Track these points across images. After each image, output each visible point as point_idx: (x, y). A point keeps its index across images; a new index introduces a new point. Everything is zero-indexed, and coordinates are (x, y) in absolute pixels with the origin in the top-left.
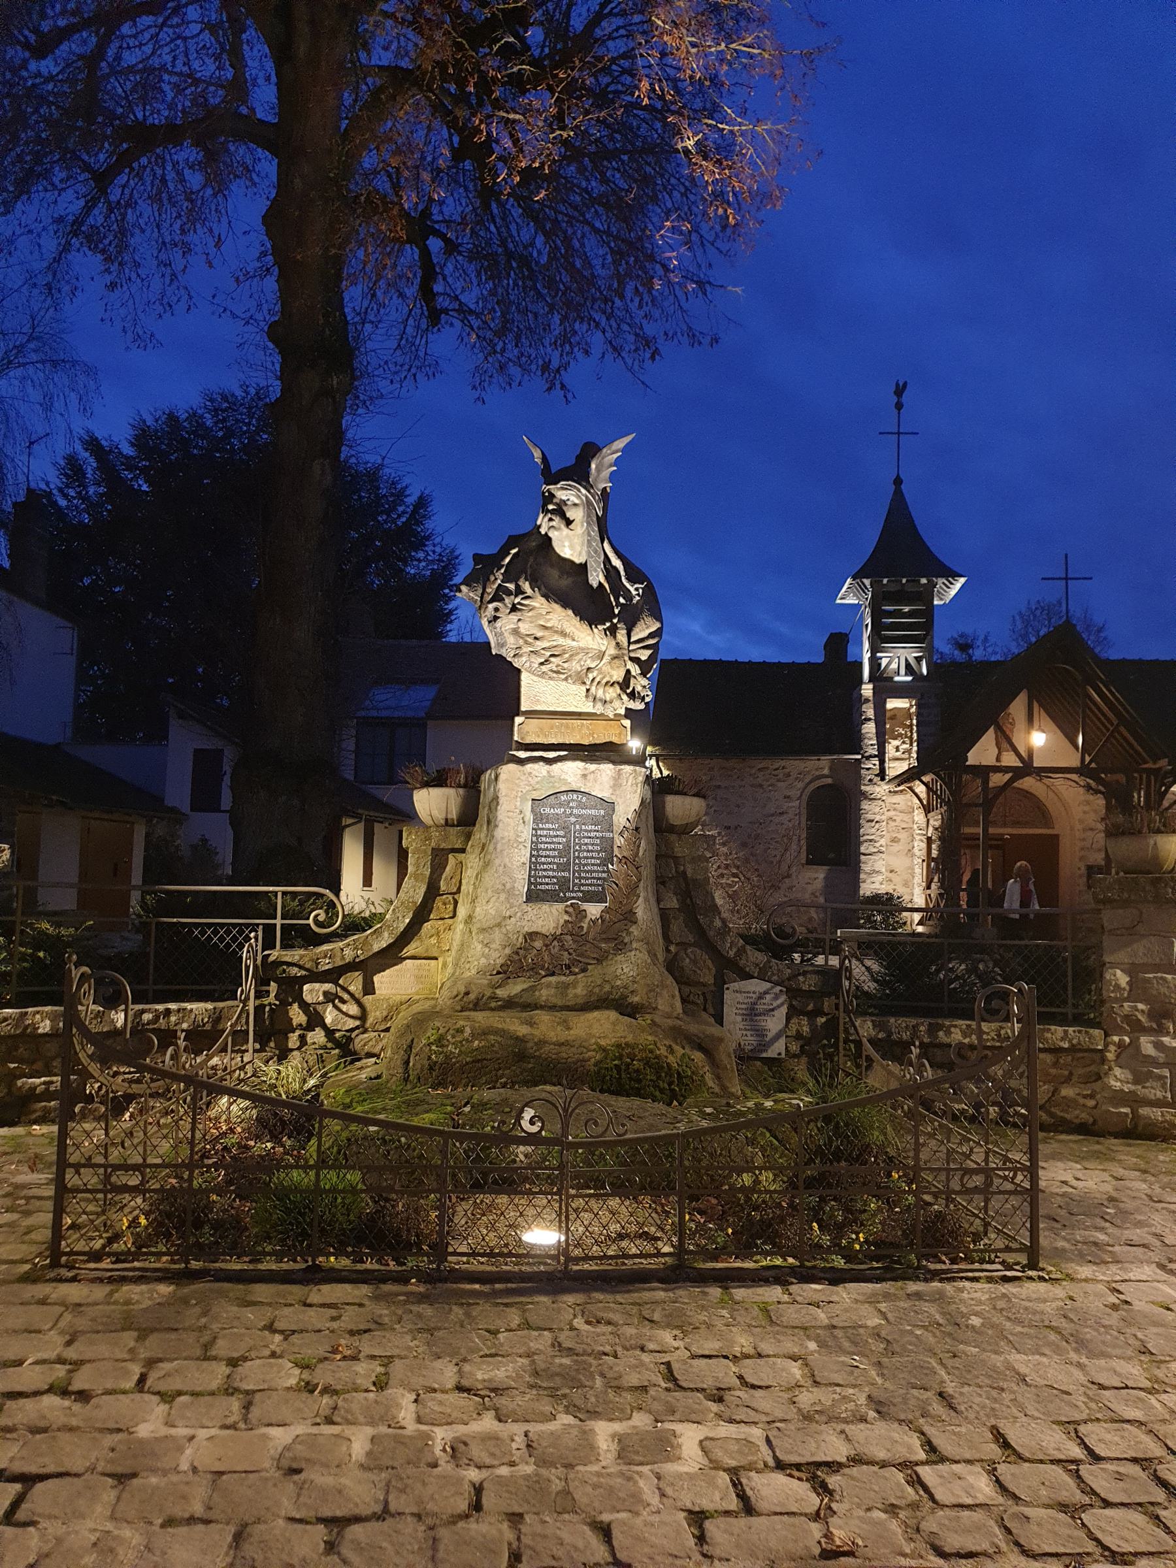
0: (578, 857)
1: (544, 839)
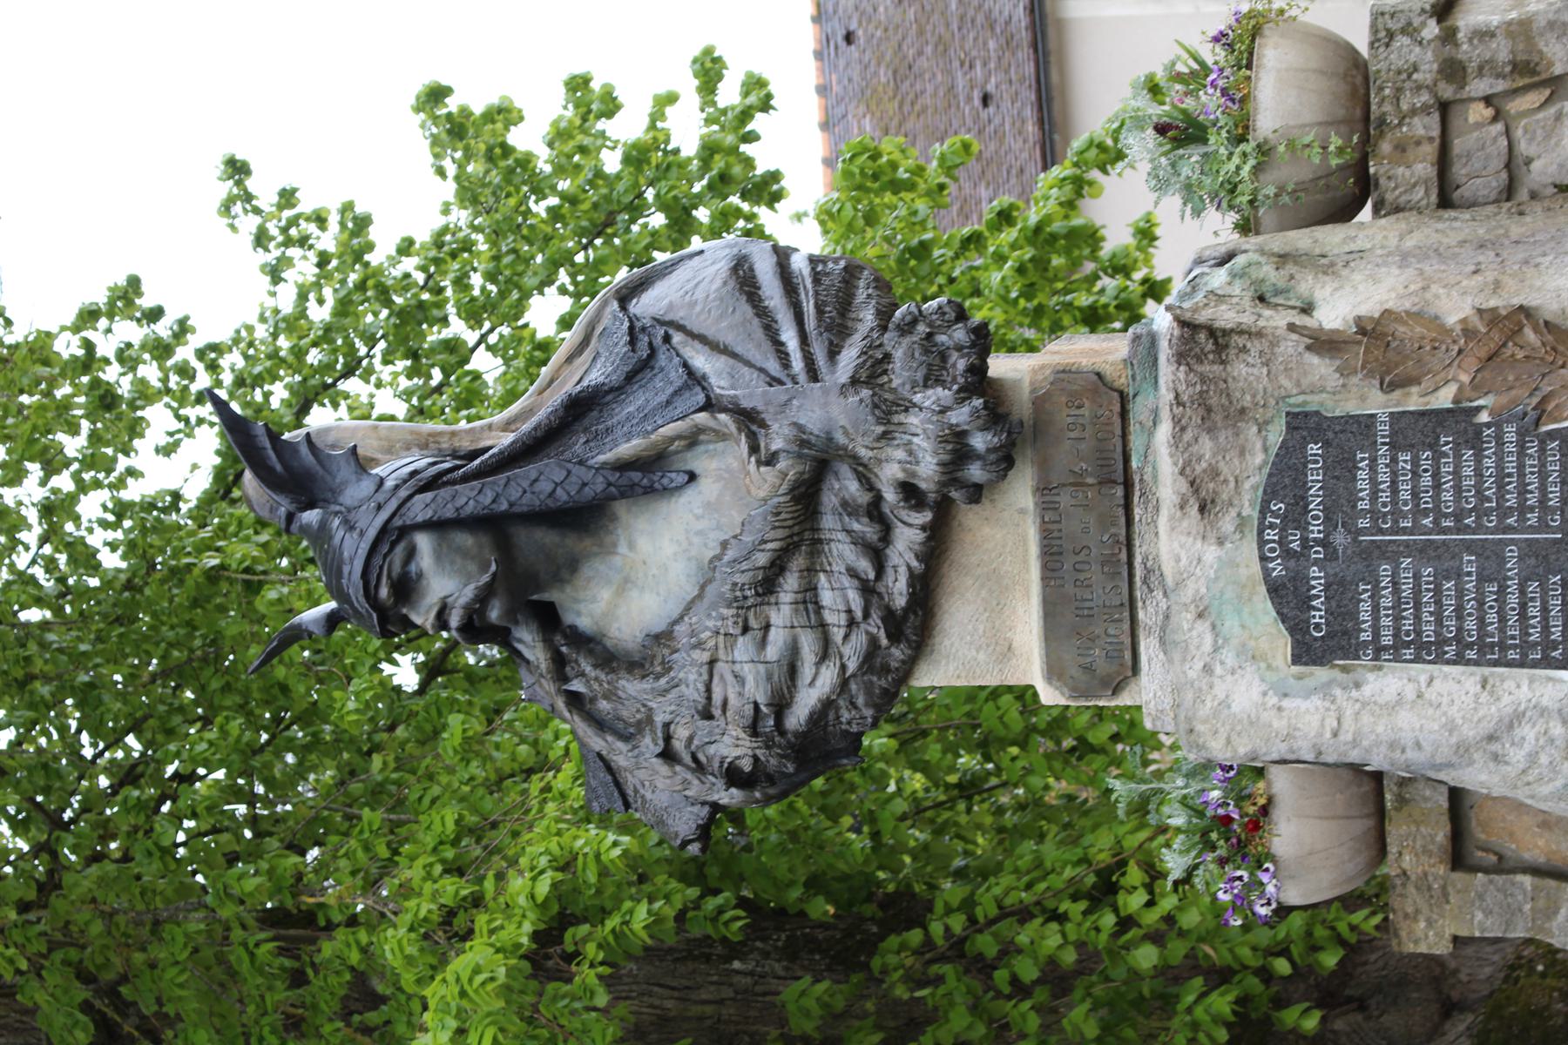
0: (1458, 516)
1: (1407, 625)
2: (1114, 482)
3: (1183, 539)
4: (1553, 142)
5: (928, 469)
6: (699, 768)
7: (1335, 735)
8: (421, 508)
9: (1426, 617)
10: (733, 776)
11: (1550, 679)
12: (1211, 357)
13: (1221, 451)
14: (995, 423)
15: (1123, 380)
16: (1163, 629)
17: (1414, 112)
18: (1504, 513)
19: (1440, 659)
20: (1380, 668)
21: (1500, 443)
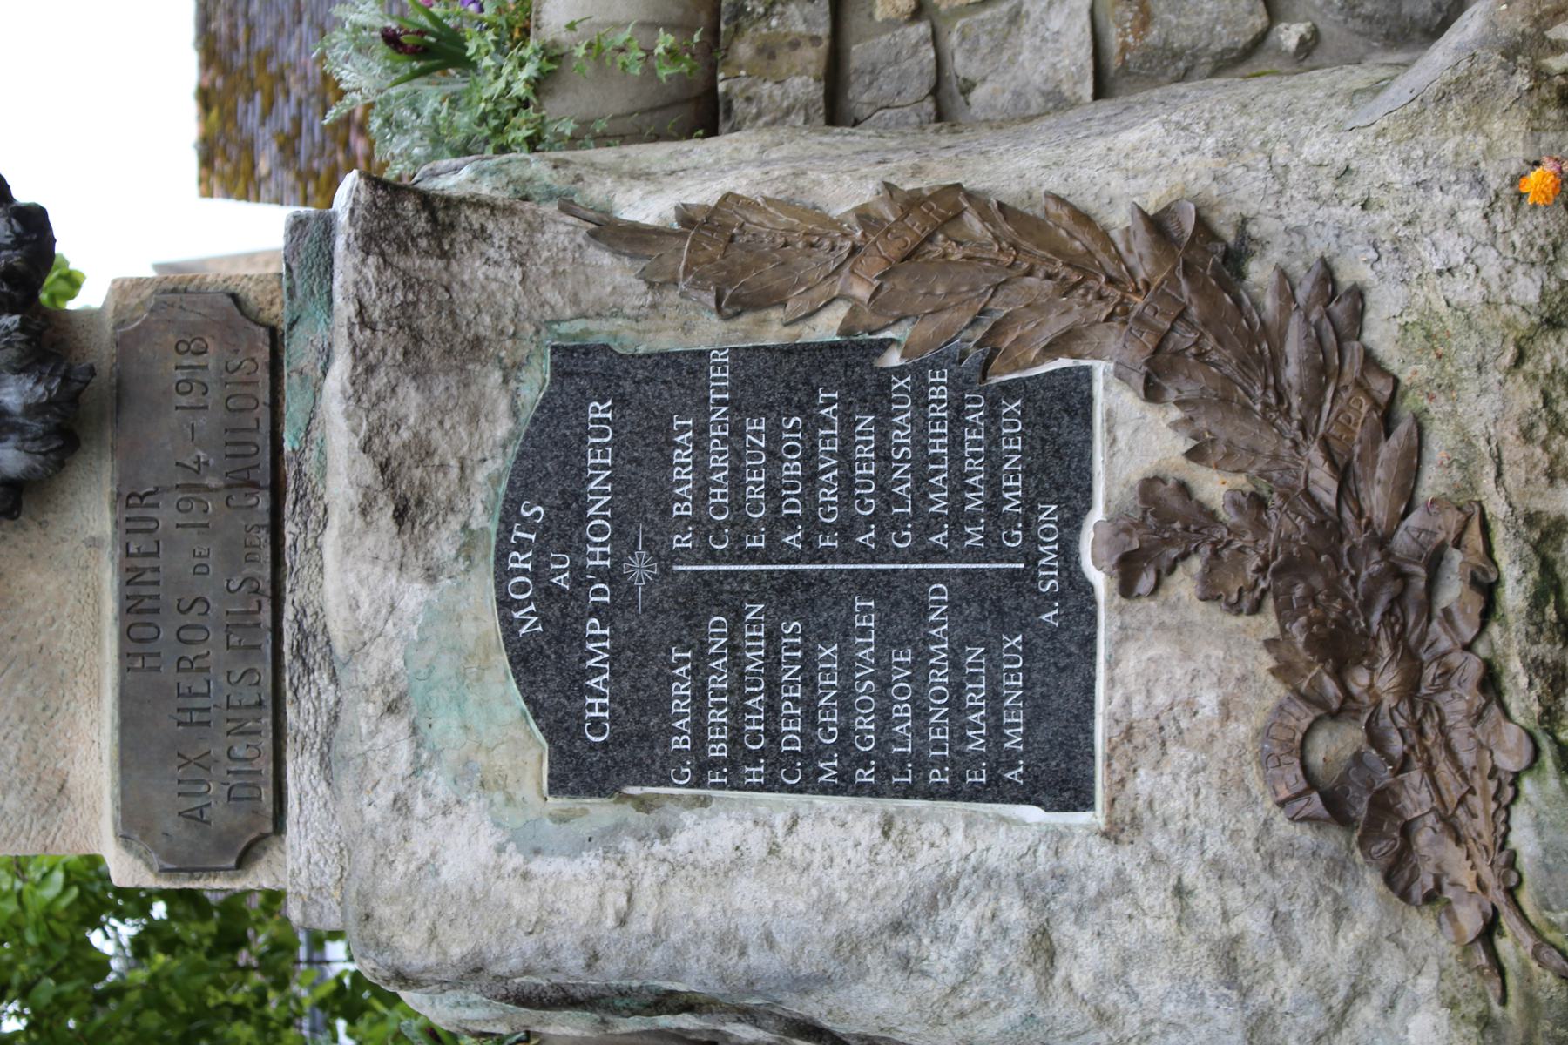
0: (846, 530)
2: (255, 485)
3: (365, 569)
4: (1005, 55)
7: (622, 922)
9: (787, 709)
11: (1002, 819)
12: (423, 243)
14: (42, 361)
15: (276, 309)
16: (327, 741)
18: (929, 525)
19: (810, 785)
20: (704, 802)
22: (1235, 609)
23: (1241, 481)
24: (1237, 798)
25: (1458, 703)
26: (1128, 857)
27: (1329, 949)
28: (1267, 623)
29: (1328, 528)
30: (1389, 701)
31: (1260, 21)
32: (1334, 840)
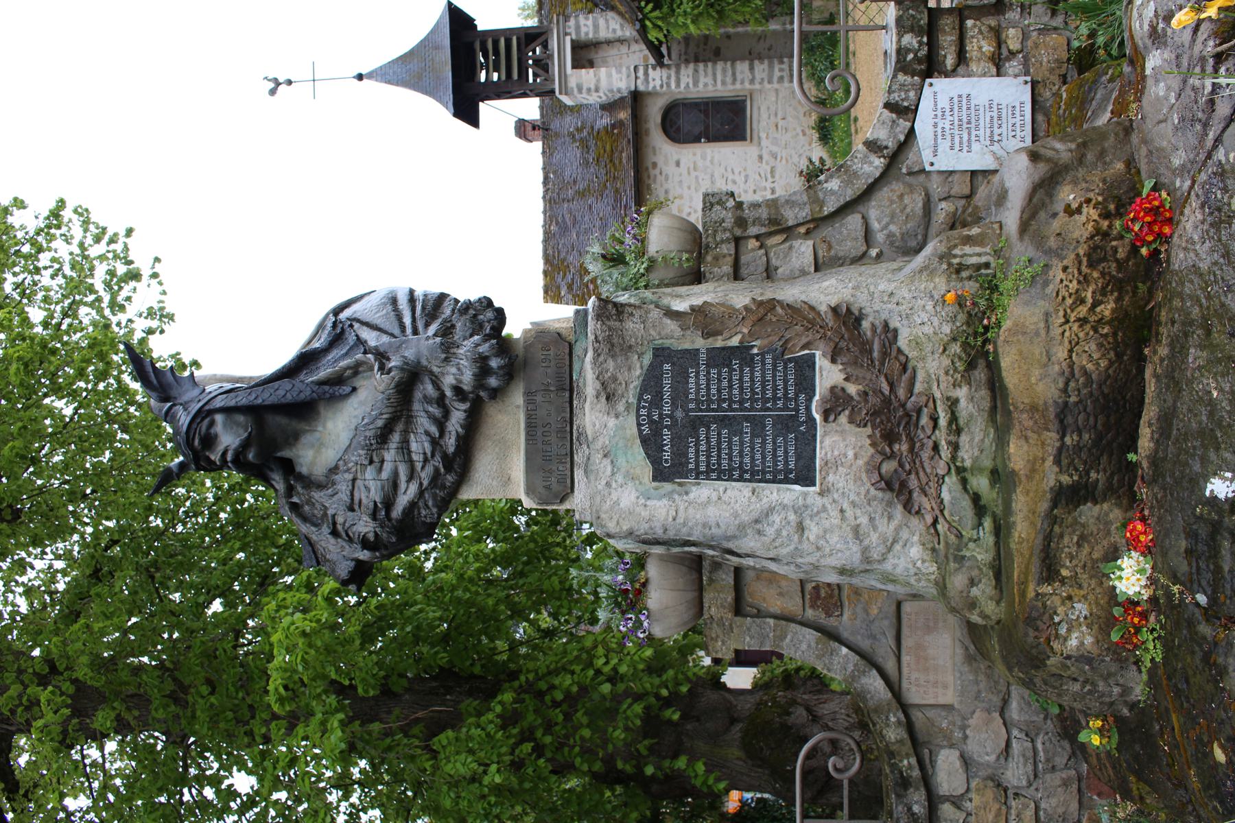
0: (741, 402)
5: (467, 378)
6: (350, 540)
8: (218, 403)
9: (723, 456)
10: (365, 544)
13: (618, 367)
16: (586, 465)
17: (722, 241)
18: (767, 400)
19: (730, 479)
20: (699, 484)
21: (764, 364)
22: (859, 426)
23: (860, 387)
24: (859, 483)
25: (926, 454)
26: (826, 501)
27: (886, 528)
28: (869, 430)
29: (887, 402)
30: (905, 454)
31: (864, 248)
32: (888, 495)
